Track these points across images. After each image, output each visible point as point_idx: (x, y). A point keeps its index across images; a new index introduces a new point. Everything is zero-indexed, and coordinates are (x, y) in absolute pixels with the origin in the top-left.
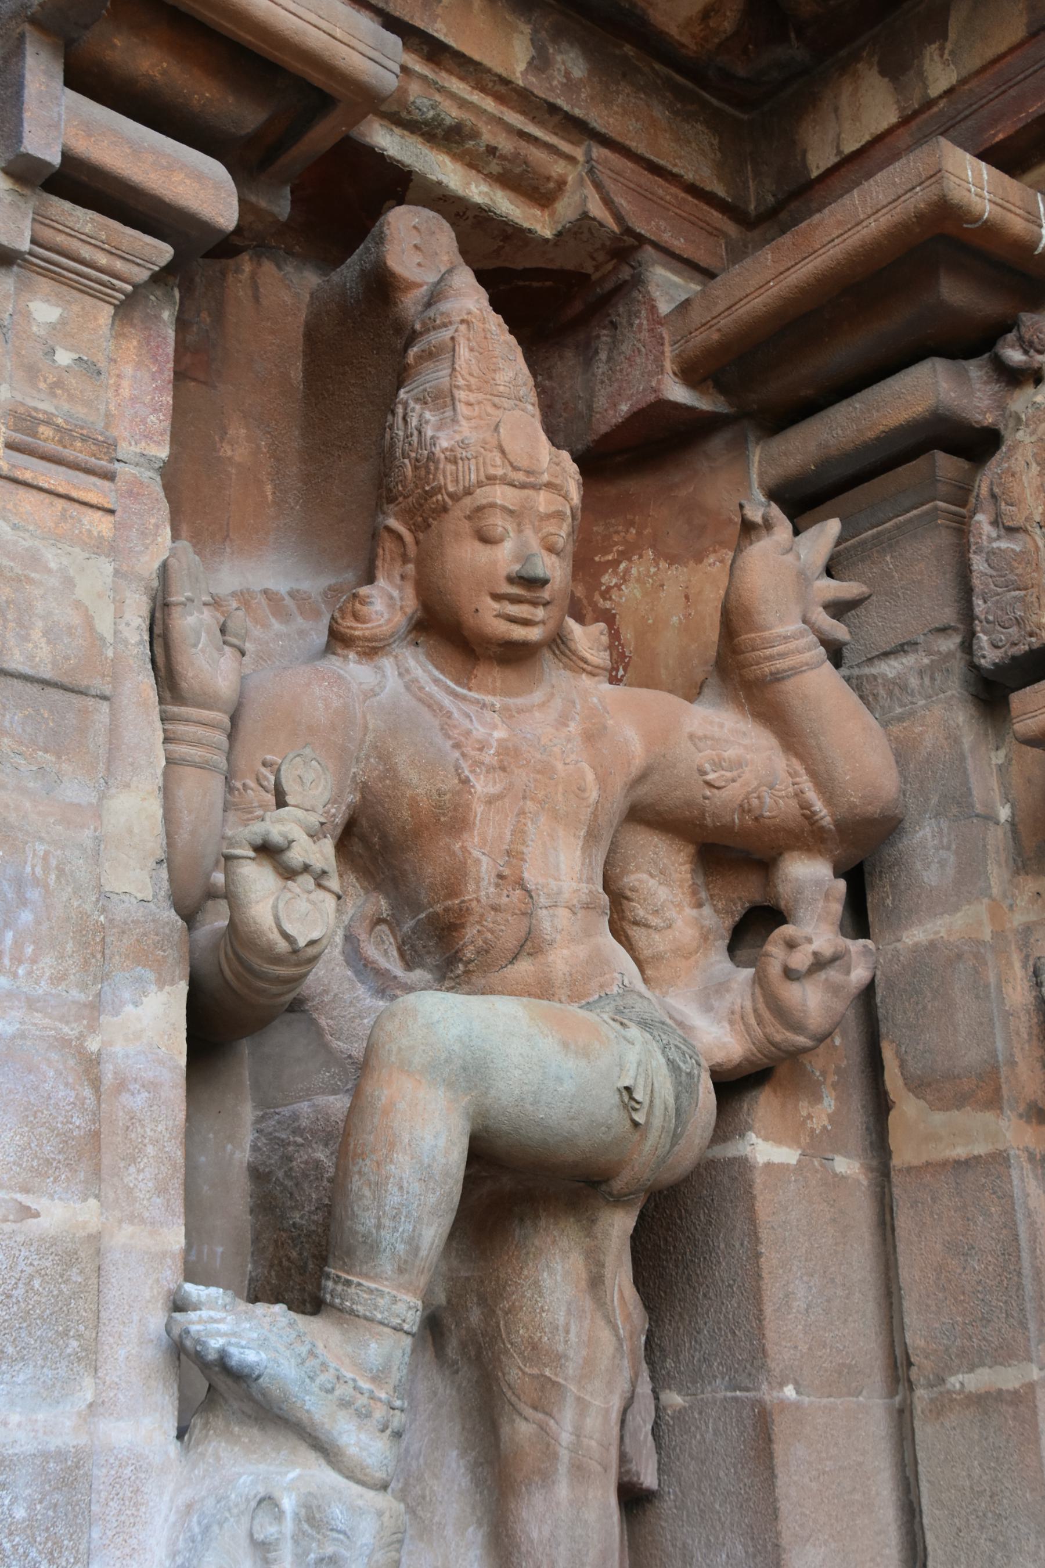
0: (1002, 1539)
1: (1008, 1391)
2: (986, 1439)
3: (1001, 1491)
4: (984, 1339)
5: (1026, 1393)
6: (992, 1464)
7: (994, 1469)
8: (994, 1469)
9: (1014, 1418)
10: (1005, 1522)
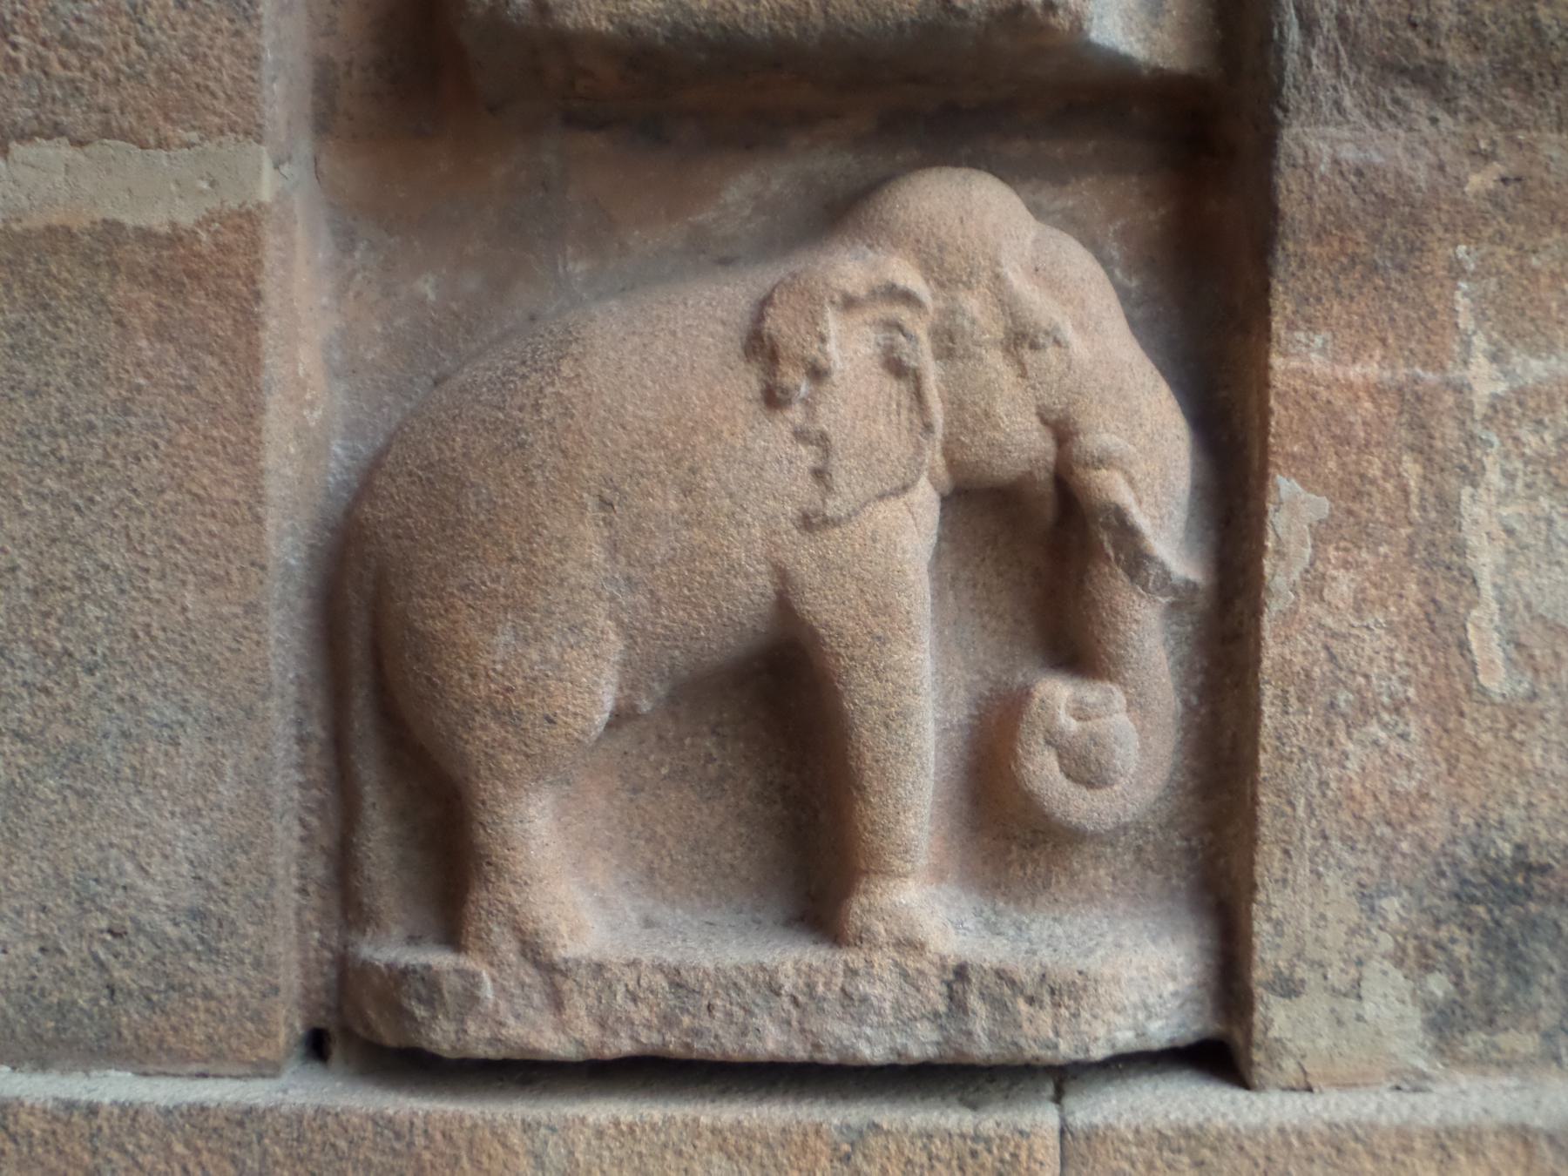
0: (66, 735)
1: (146, 236)
2: (33, 393)
3: (81, 578)
4: (67, 41)
5: (225, 249)
6: (51, 483)
7: (58, 500)
8: (58, 500)
9: (160, 332)
10: (86, 681)
